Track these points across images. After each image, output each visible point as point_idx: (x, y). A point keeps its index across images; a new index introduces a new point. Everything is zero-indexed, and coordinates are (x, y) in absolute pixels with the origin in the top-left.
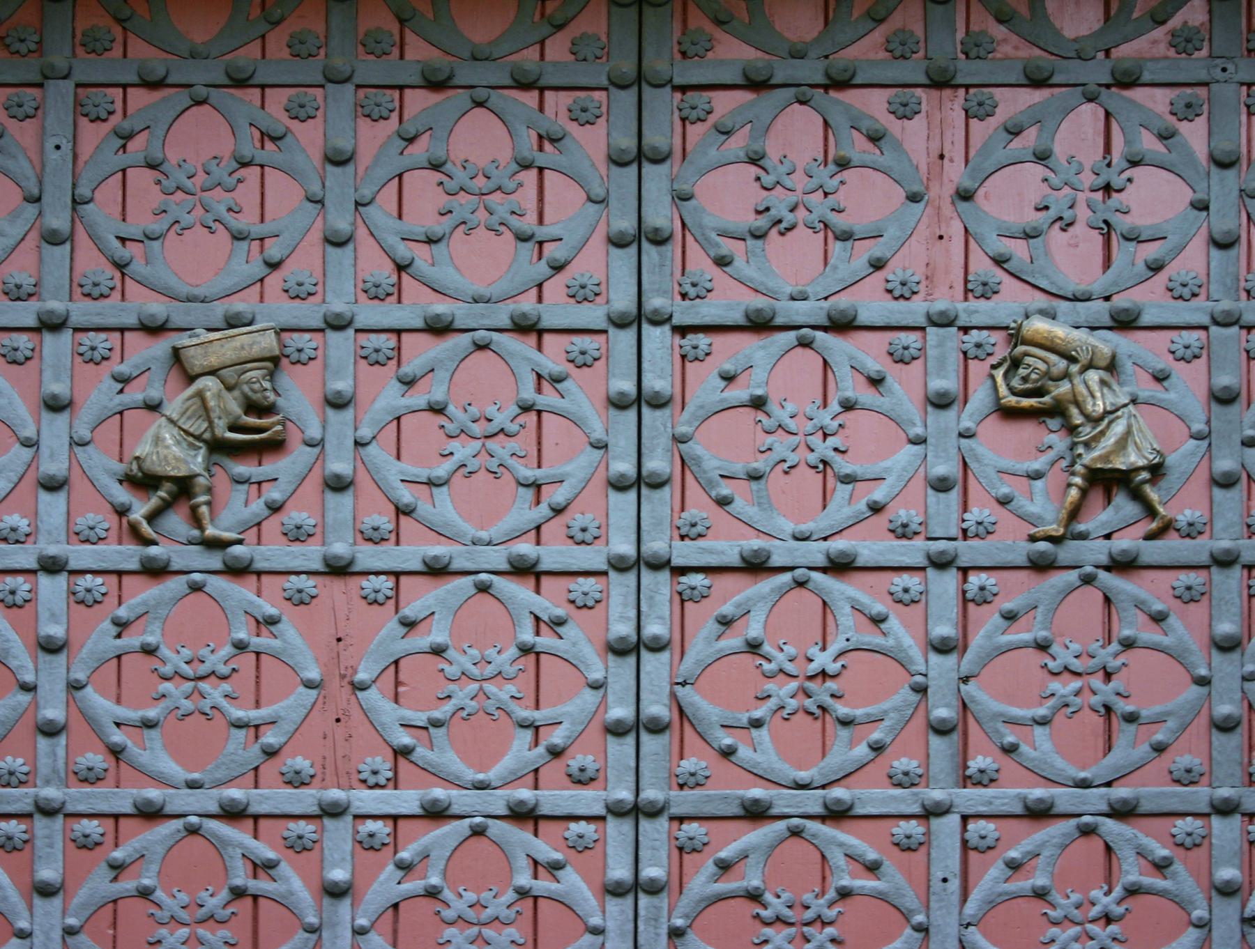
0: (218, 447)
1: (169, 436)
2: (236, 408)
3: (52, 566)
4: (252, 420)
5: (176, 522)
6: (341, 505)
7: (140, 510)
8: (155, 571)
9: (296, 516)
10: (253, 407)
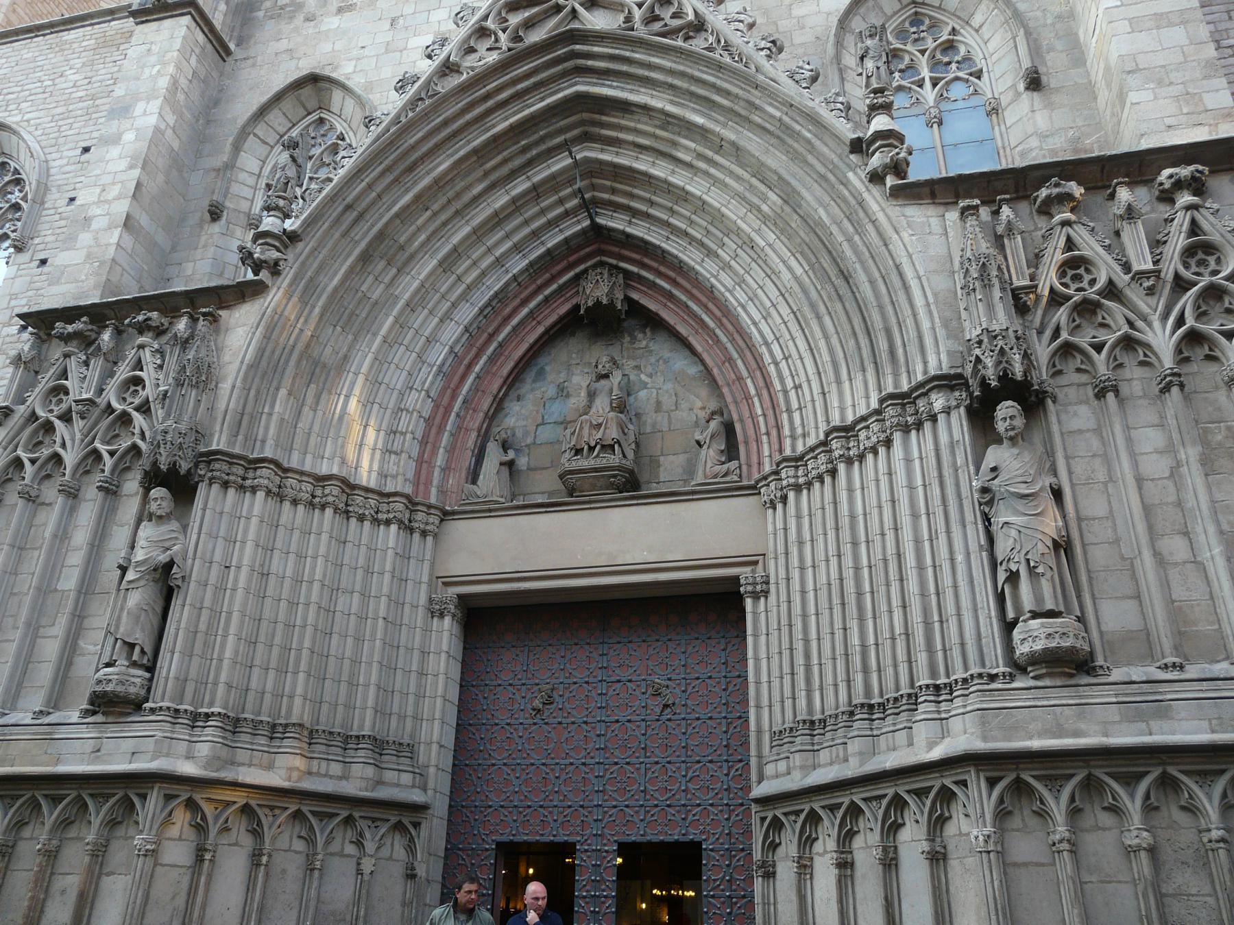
0: (544, 704)
8: (535, 724)
10: (550, 697)
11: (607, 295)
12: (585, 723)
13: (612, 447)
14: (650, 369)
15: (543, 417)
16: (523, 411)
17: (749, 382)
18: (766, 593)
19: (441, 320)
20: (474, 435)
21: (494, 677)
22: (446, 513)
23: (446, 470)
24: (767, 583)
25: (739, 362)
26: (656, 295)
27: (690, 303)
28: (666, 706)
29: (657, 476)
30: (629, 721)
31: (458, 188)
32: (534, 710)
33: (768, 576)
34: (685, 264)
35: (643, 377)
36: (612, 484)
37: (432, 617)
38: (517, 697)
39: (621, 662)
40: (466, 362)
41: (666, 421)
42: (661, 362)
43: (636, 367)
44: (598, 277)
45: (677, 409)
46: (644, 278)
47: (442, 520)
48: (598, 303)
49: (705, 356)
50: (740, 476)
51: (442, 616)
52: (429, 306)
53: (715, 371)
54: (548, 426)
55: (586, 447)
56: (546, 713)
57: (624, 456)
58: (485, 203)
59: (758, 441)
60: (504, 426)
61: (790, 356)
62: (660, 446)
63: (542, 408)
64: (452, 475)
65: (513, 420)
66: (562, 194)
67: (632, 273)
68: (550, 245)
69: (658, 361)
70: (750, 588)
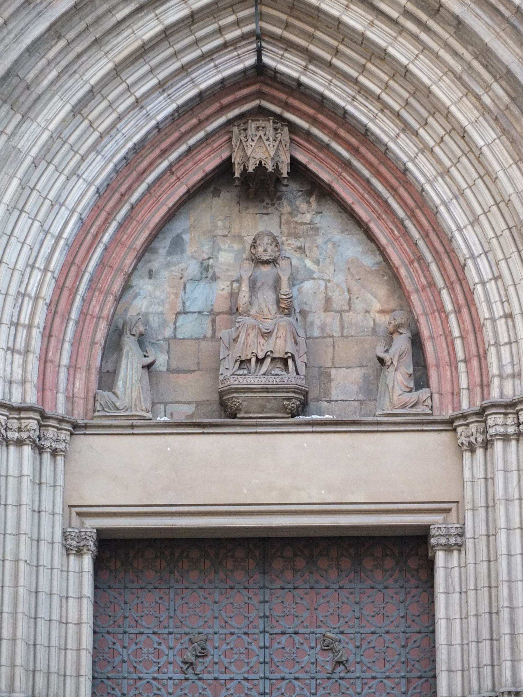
0: (197, 656)
1: (189, 654)
2: (200, 649)
3: (170, 679)
4: (202, 651)
5: (190, 670)
6: (217, 667)
7: (185, 667)
8: (187, 679)
9: (210, 669)
11: (273, 159)
12: (246, 679)
13: (285, 361)
14: (316, 253)
15: (184, 303)
16: (158, 293)
17: (445, 293)
18: (460, 547)
19: (68, 179)
20: (103, 326)
21: (134, 624)
22: (75, 426)
23: (72, 368)
24: (461, 535)
25: (433, 267)
26: (329, 161)
27: (375, 181)
28: (339, 663)
29: (328, 392)
30: (296, 679)
31: (100, 11)
32: (185, 663)
33: (463, 527)
34: (373, 134)
35: (308, 263)
36: (285, 407)
37: (68, 555)
38: (163, 647)
39: (286, 612)
40: (93, 231)
41: (337, 323)
42: (330, 245)
43: (300, 248)
44: (261, 133)
45: (350, 310)
46: (316, 136)
47: (72, 434)
48: (260, 167)
49: (390, 250)
50: (432, 408)
51: (79, 553)
52: (56, 161)
53: (403, 272)
54: (190, 317)
55: (254, 360)
56: (199, 668)
57: (297, 373)
58: (130, 31)
59: (454, 365)
60: (132, 312)
61: (500, 277)
62: (331, 355)
63: (182, 292)
64: (78, 376)
65: (145, 304)
66: (223, 22)
67: (300, 128)
68: (203, 86)
69: (326, 243)
70: (443, 541)
